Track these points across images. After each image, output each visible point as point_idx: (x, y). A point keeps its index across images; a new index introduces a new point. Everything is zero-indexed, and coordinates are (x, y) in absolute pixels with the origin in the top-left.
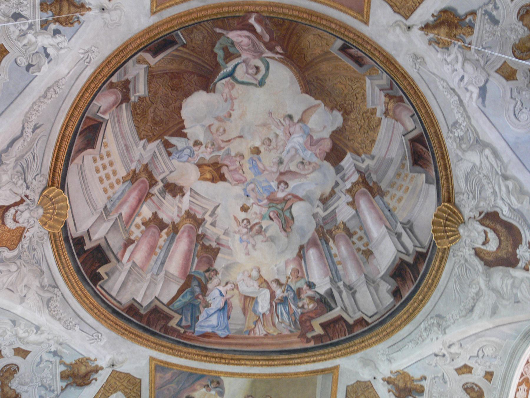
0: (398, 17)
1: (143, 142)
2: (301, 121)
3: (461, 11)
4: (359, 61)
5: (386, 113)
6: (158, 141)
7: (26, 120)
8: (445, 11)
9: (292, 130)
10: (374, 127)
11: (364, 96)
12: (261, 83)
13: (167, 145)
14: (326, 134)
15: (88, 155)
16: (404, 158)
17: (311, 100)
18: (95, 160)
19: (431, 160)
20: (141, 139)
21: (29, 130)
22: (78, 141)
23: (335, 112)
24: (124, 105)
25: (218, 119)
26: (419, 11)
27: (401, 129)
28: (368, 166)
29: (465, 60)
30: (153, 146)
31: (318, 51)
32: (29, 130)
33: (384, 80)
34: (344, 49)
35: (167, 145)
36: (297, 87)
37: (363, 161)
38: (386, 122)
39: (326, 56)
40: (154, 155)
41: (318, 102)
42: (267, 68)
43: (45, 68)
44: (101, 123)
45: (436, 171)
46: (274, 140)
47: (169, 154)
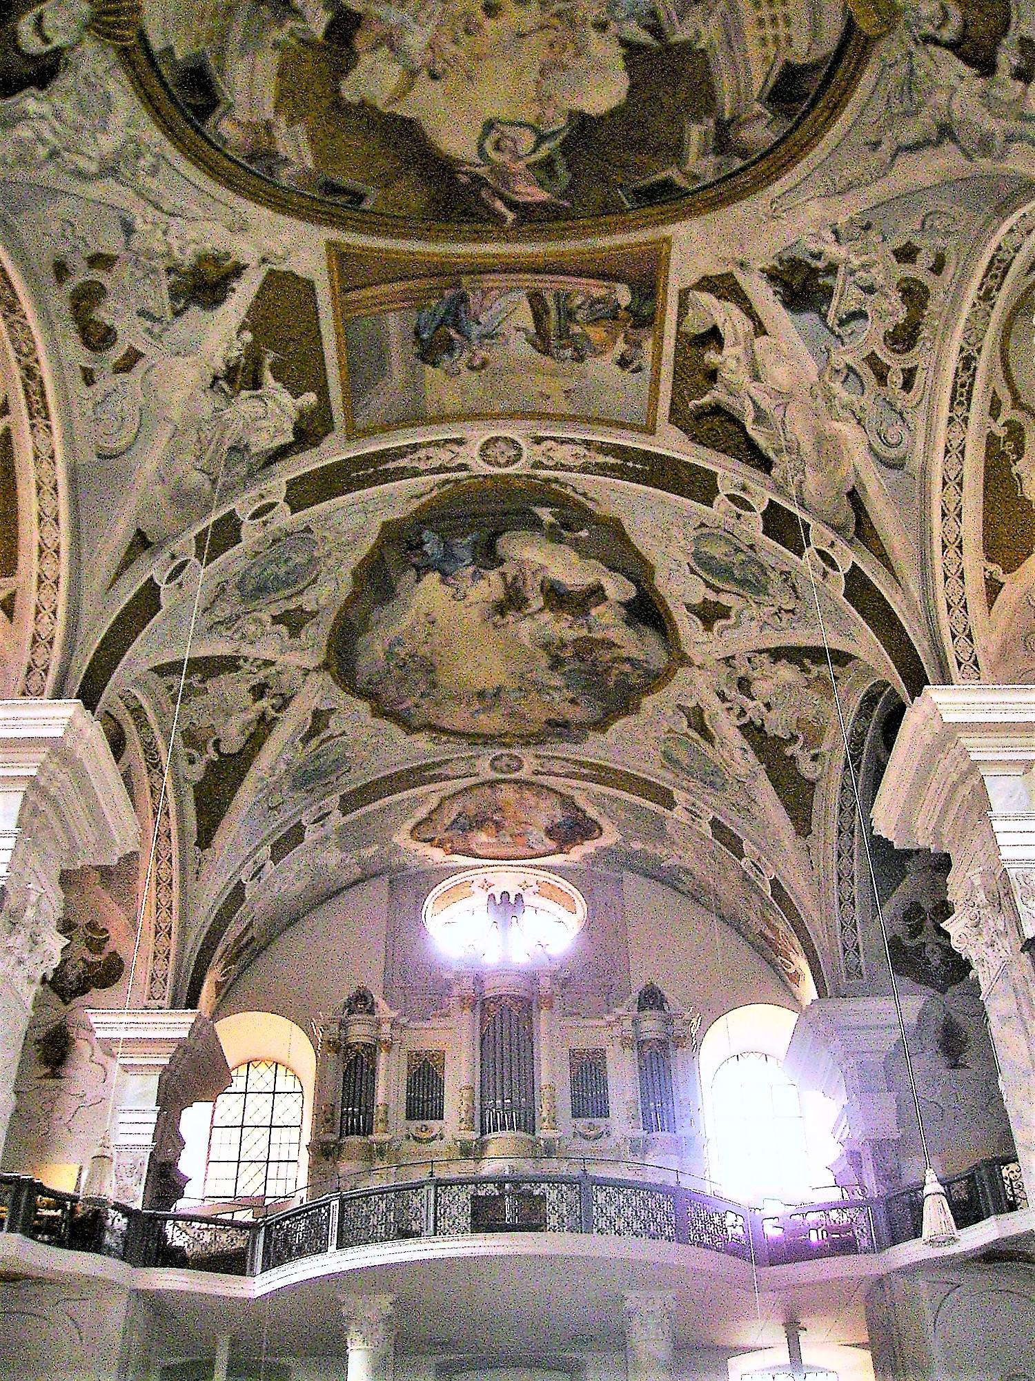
0: (284, 268)
1: (701, 45)
2: (413, 74)
3: (195, 309)
4: (332, 188)
5: (268, 127)
6: (674, 39)
7: (884, 171)
8: (218, 302)
9: (429, 55)
10: (282, 97)
11: (312, 139)
12: (490, 126)
13: (656, 30)
14: (366, 60)
15: (801, 51)
16: (221, 71)
17: (400, 110)
18: (789, 40)
19: (174, 91)
20: (702, 50)
21: (886, 148)
22: (812, 87)
23: (356, 99)
24: (727, 116)
25: (564, 68)
26: (255, 289)
27: (241, 115)
28: (281, 26)
29: (169, 254)
30: (680, 35)
31: (402, 185)
32: (886, 148)
33: (284, 176)
34: (359, 198)
35: (656, 30)
36: (428, 125)
37: (292, 34)
38: (268, 112)
39: (386, 182)
40: (681, 17)
41: (386, 111)
42: (481, 147)
43: (842, 220)
44: (769, 99)
45: (160, 77)
46: (461, 34)
47: (653, 14)
